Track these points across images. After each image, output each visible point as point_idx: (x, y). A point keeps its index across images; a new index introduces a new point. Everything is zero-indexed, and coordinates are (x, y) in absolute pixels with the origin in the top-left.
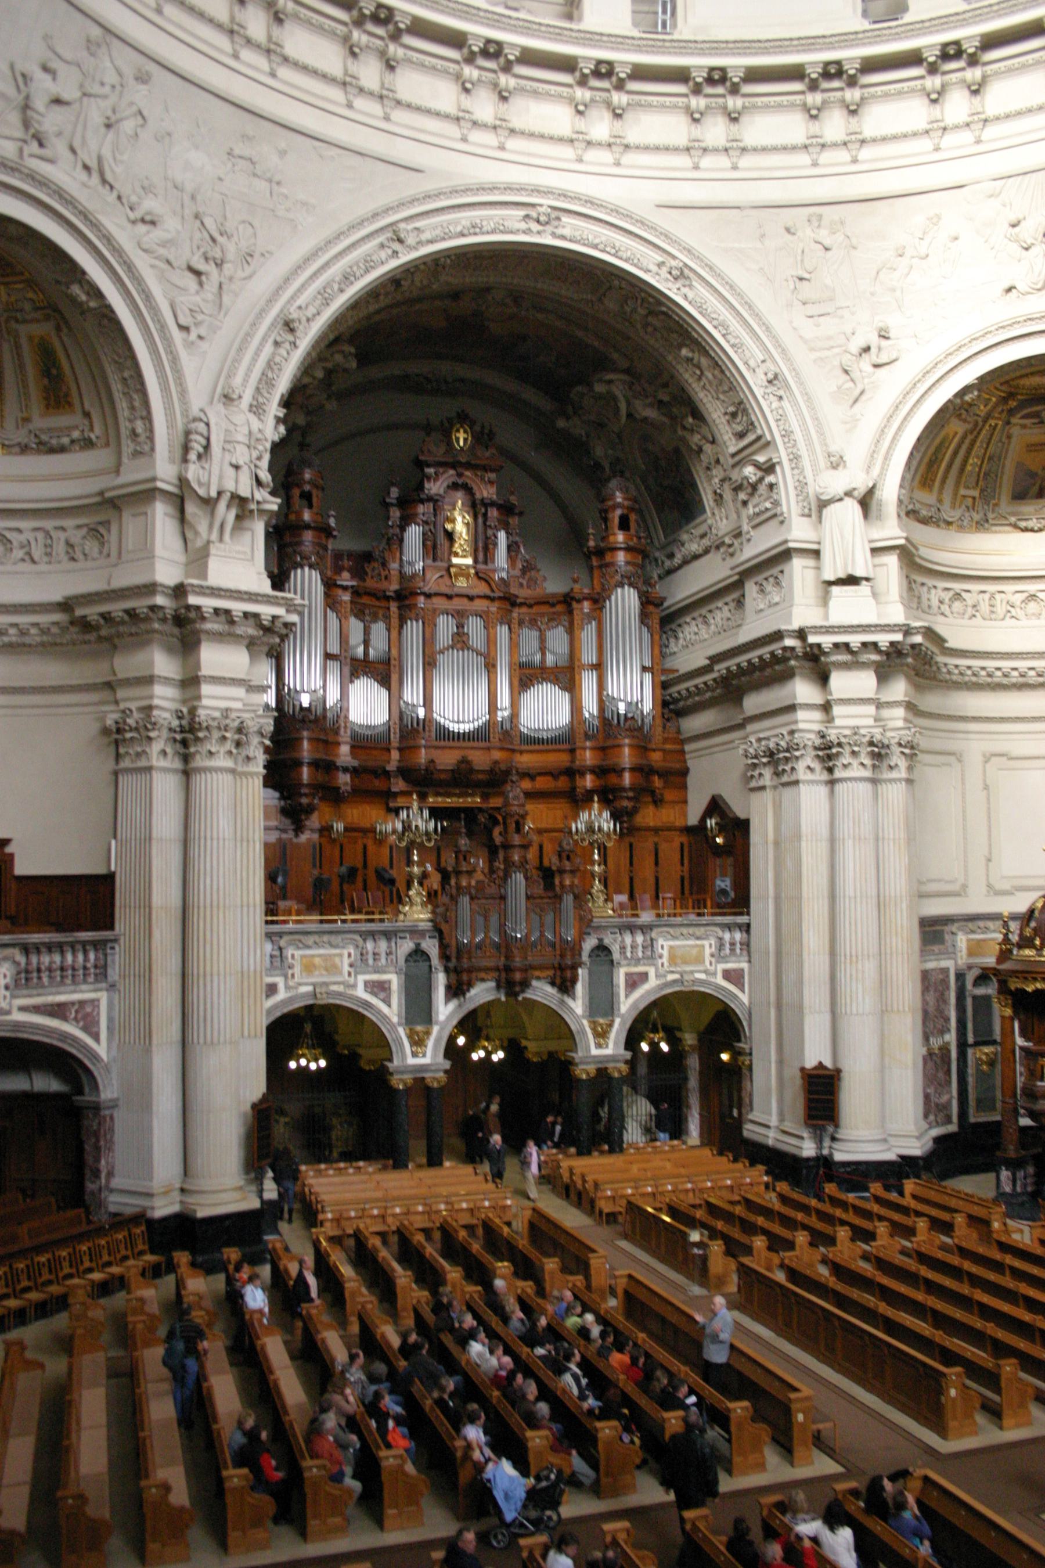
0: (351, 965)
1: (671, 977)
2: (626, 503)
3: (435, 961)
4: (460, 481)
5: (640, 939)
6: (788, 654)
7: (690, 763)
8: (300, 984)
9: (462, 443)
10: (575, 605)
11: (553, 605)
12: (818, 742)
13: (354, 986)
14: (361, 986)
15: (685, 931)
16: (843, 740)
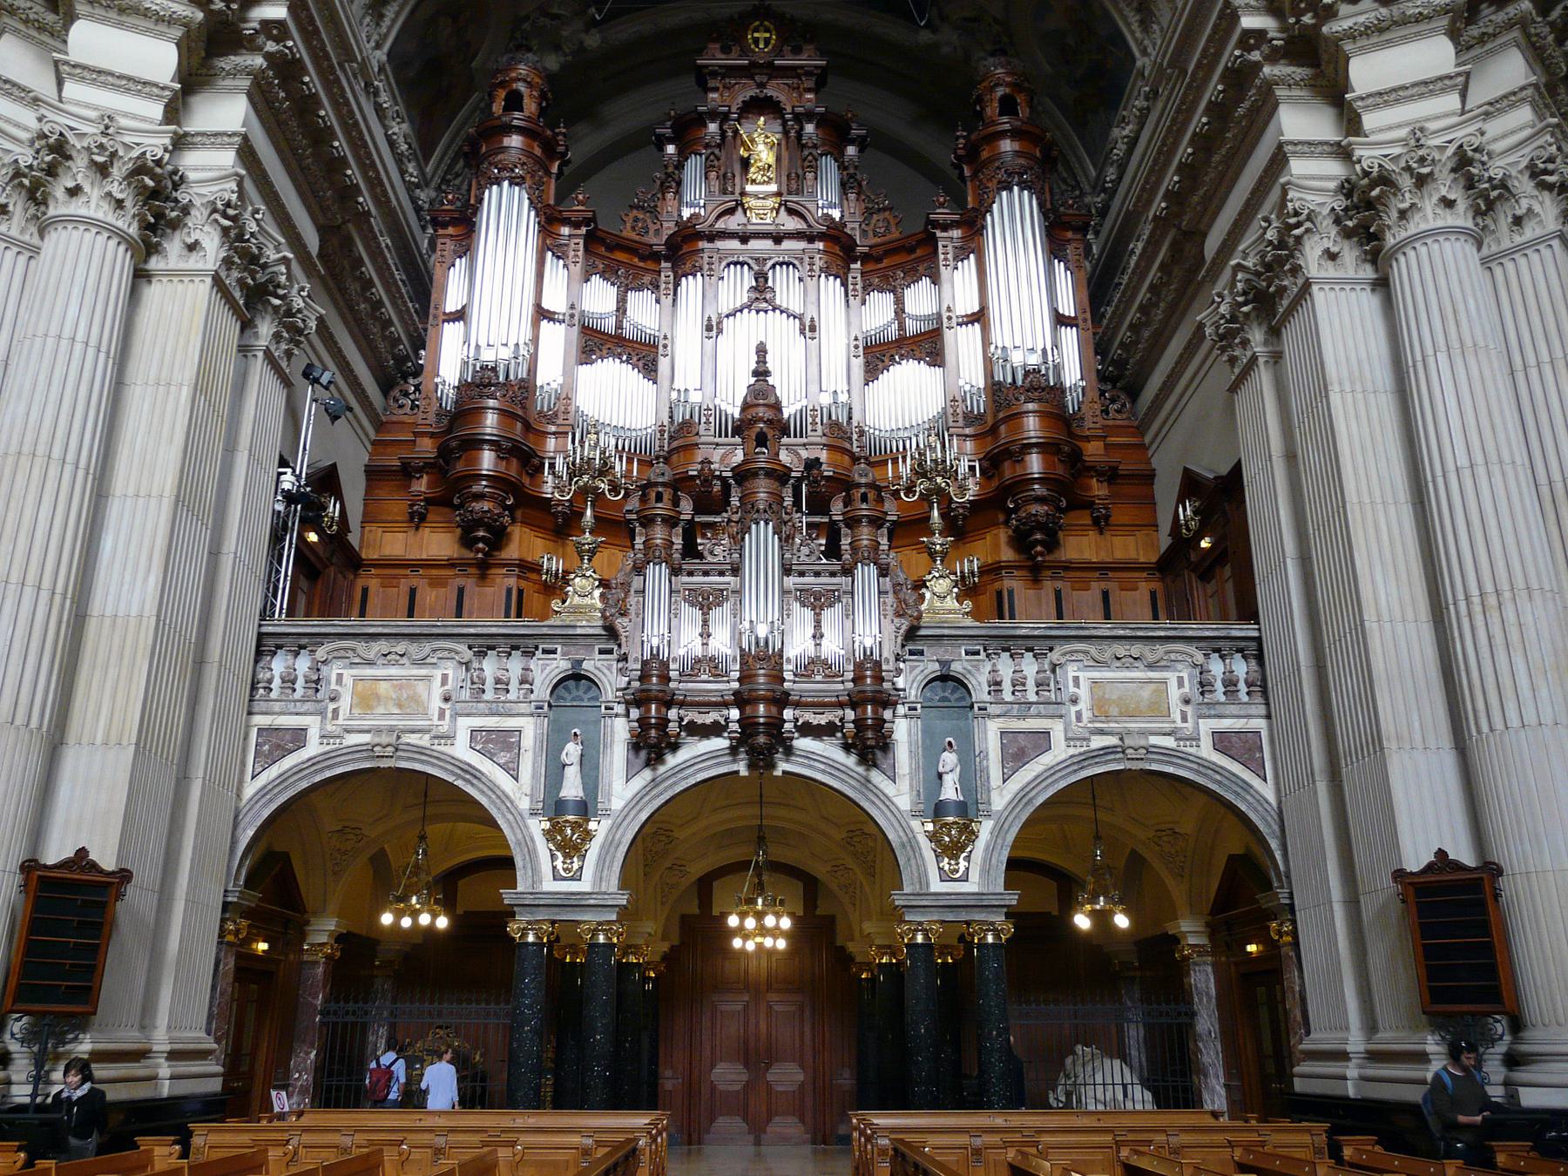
0: (447, 700)
1: (1097, 742)
2: (1008, 79)
3: (609, 694)
4: (762, 96)
5: (1030, 667)
6: (1256, 56)
7: (1155, 463)
8: (348, 732)
9: (761, 46)
10: (939, 234)
11: (911, 250)
12: (1339, 203)
13: (449, 737)
14: (463, 738)
15: (1120, 649)
16: (1389, 166)
